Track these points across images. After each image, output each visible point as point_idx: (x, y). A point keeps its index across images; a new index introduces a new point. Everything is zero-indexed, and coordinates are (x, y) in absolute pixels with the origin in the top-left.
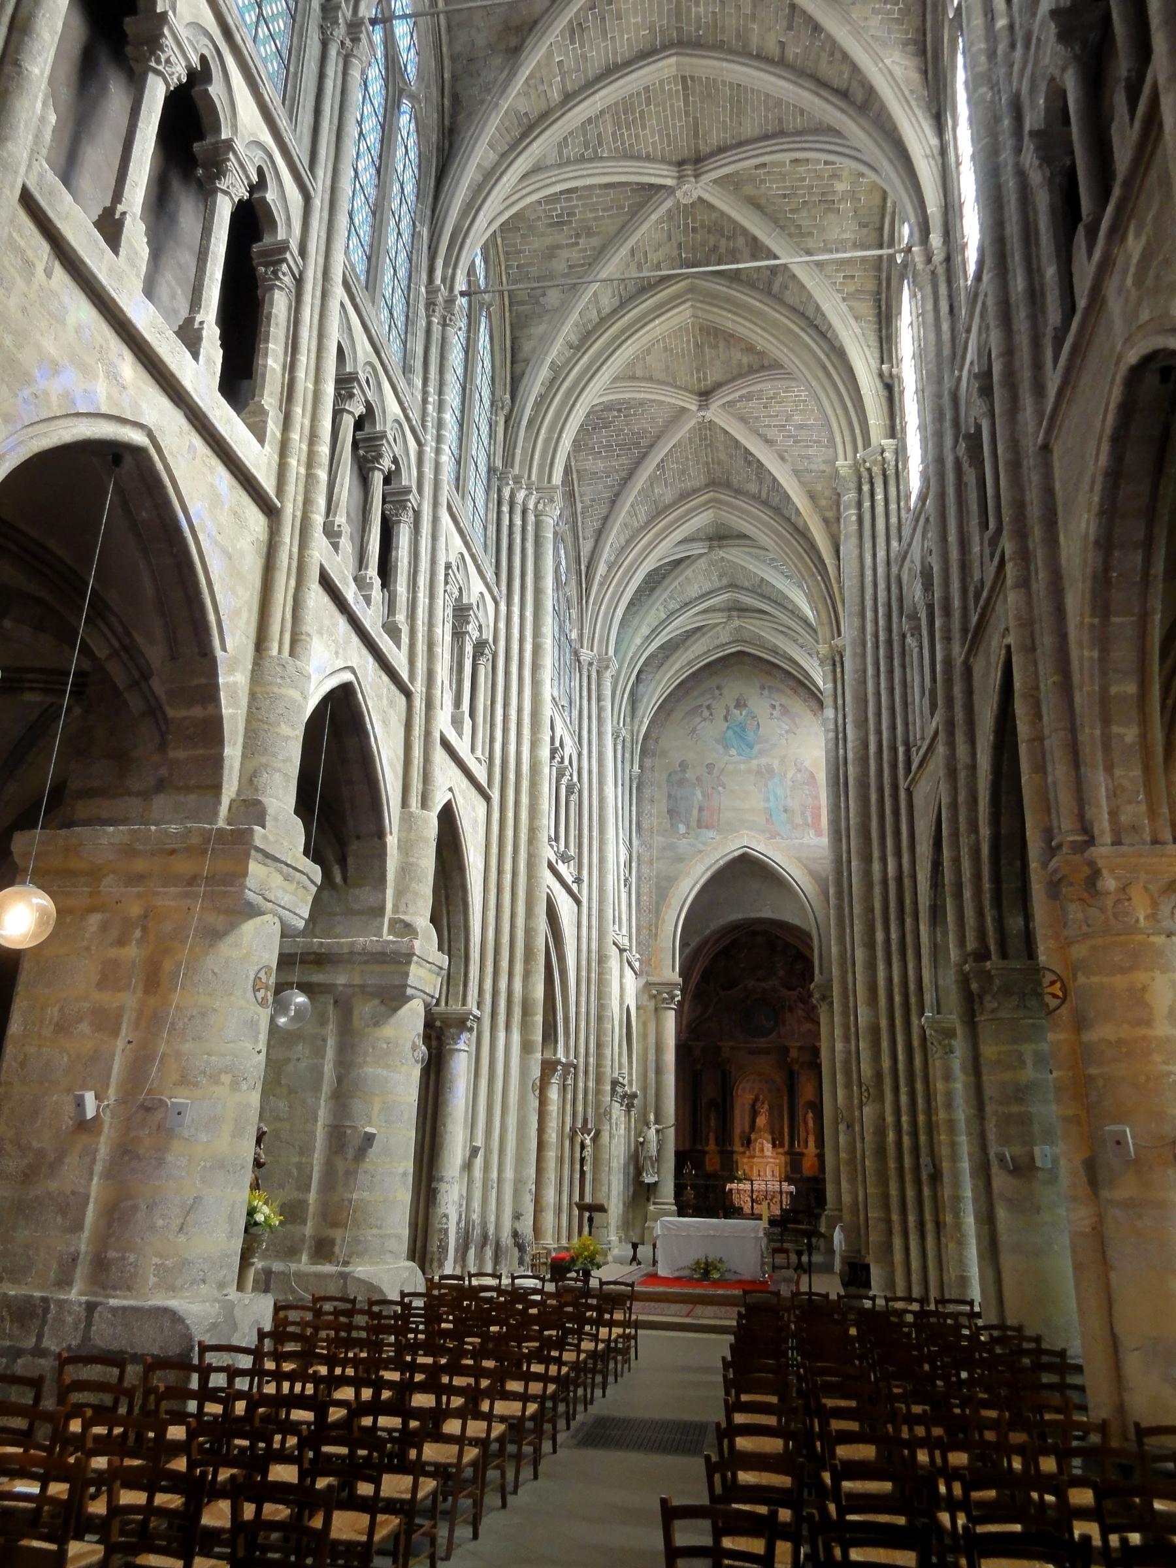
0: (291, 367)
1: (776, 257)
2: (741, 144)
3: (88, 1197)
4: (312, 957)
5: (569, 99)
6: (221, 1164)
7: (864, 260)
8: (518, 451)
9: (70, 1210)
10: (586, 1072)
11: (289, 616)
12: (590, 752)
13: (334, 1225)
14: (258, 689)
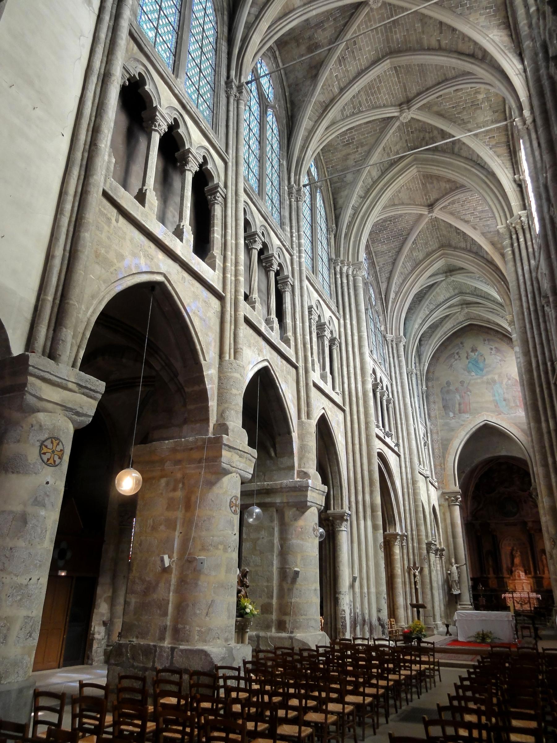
0: (225, 236)
1: (454, 137)
2: (427, 89)
3: (169, 601)
4: (265, 491)
5: (342, 90)
6: (222, 585)
7: (498, 128)
8: (342, 249)
9: (162, 606)
10: (412, 539)
11: (232, 342)
12: (396, 383)
13: (285, 614)
14: (221, 375)
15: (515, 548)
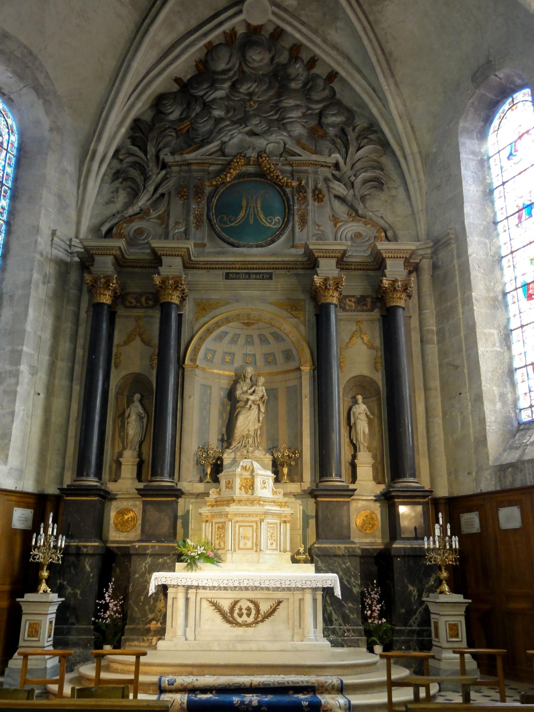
15: (250, 371)
